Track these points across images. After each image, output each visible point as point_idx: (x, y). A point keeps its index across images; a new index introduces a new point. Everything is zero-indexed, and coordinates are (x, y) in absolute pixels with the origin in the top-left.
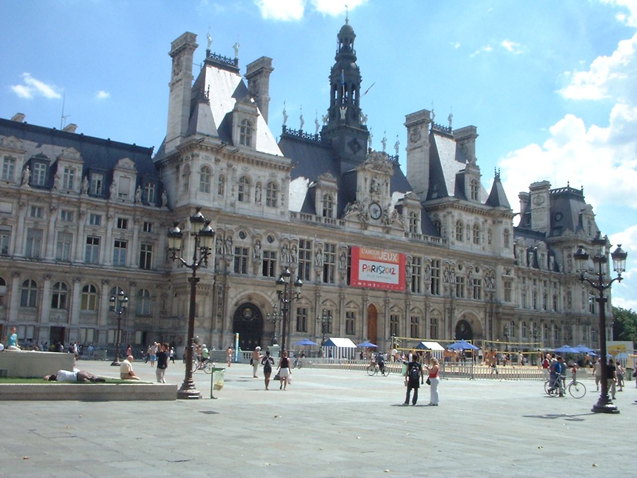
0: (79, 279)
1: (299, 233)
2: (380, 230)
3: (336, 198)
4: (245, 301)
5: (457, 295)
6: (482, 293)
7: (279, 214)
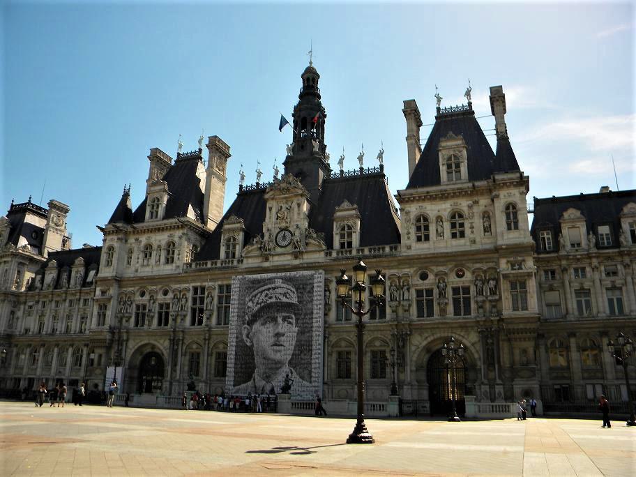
0: (72, 345)
1: (194, 281)
2: (289, 257)
3: (240, 237)
4: (148, 350)
5: (420, 314)
6: (473, 306)
7: (174, 268)
